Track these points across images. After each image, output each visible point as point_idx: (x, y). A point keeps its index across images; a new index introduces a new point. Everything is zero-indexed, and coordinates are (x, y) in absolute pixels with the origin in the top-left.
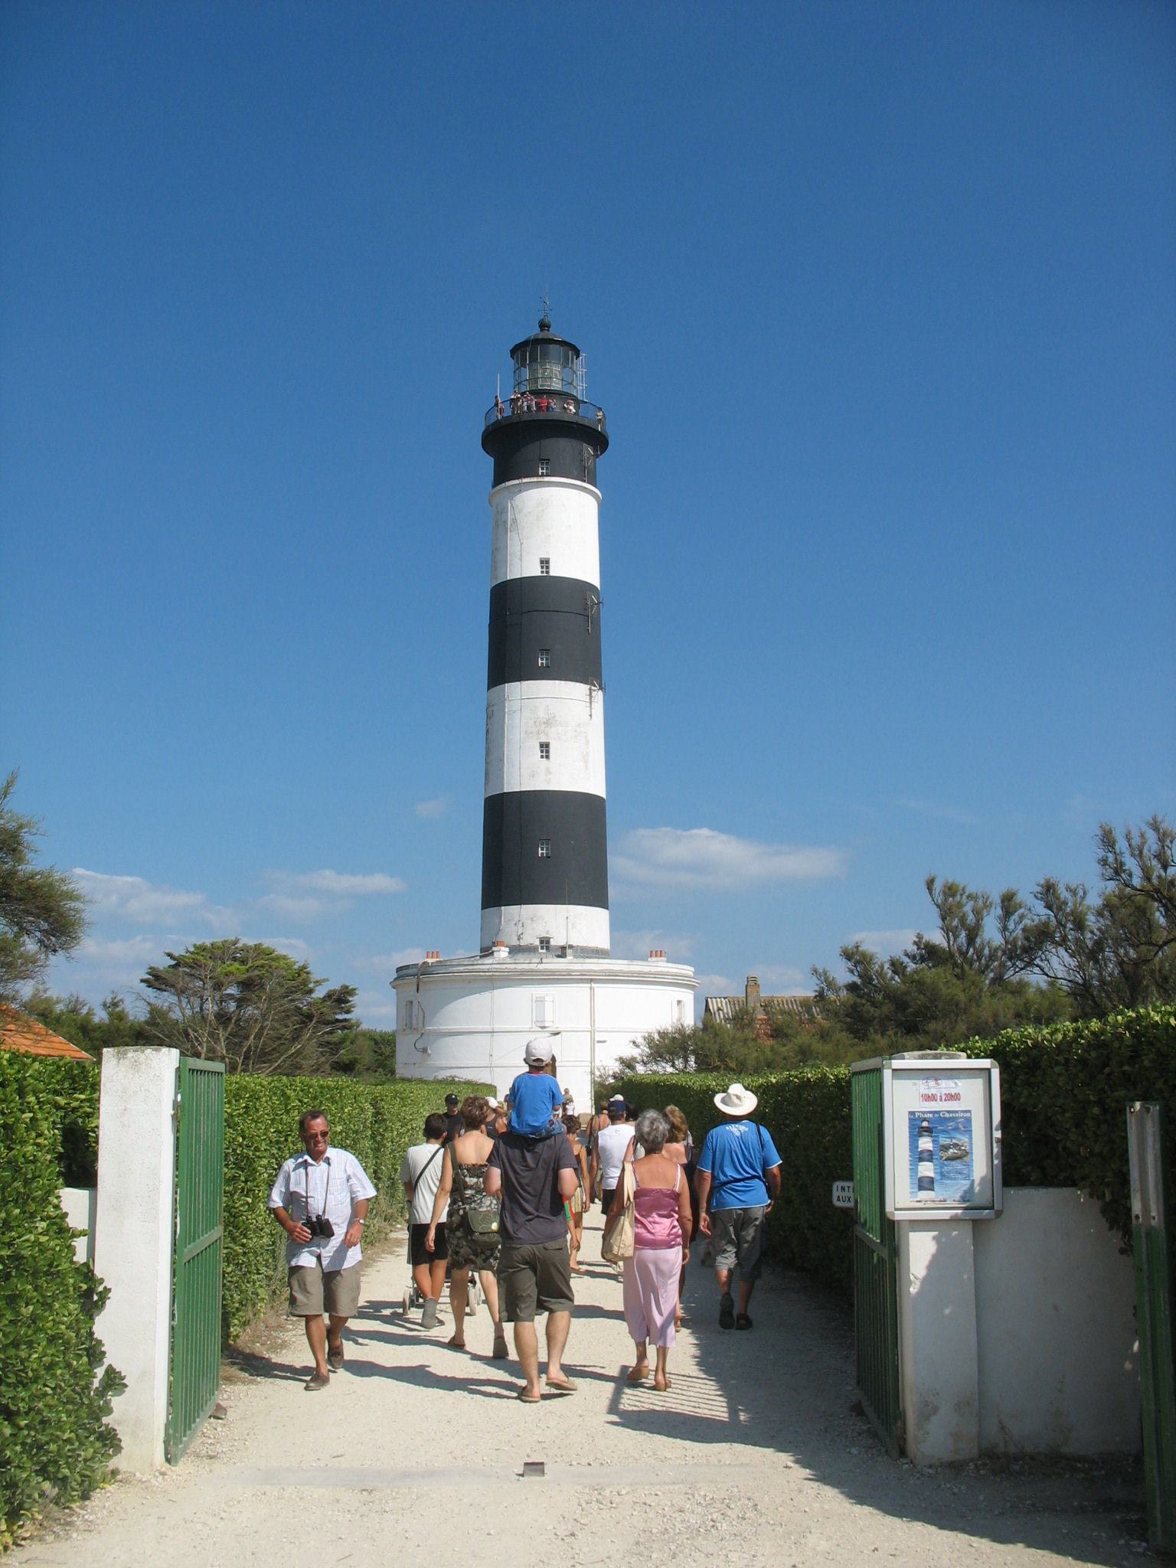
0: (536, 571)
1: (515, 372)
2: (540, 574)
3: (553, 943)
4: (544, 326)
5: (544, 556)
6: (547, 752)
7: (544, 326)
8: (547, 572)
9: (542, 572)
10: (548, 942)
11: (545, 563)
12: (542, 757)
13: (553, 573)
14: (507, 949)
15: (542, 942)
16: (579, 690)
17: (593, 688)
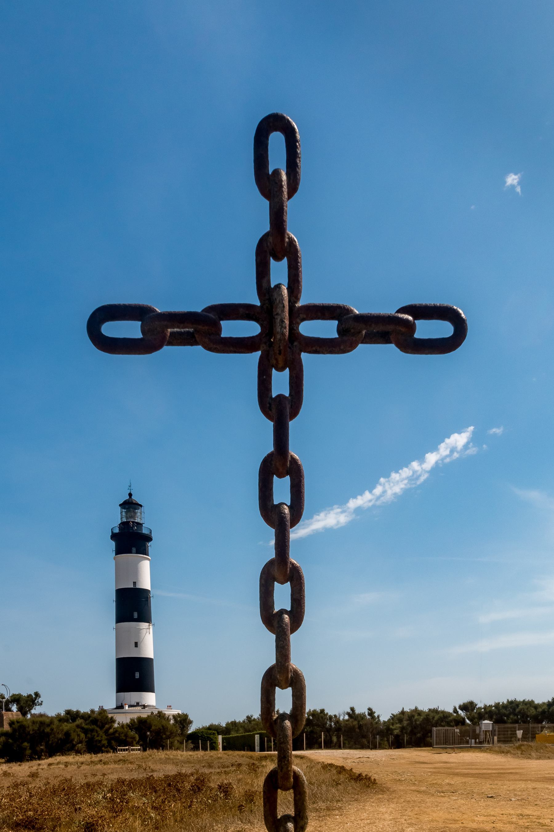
0: (132, 586)
1: (121, 513)
2: (133, 587)
3: (140, 704)
4: (130, 495)
5: (135, 581)
6: (137, 645)
7: (130, 495)
8: (135, 586)
9: (134, 586)
10: (138, 703)
11: (135, 583)
12: (135, 646)
13: (137, 587)
14: (128, 706)
15: (137, 703)
16: (147, 624)
17: (150, 624)
